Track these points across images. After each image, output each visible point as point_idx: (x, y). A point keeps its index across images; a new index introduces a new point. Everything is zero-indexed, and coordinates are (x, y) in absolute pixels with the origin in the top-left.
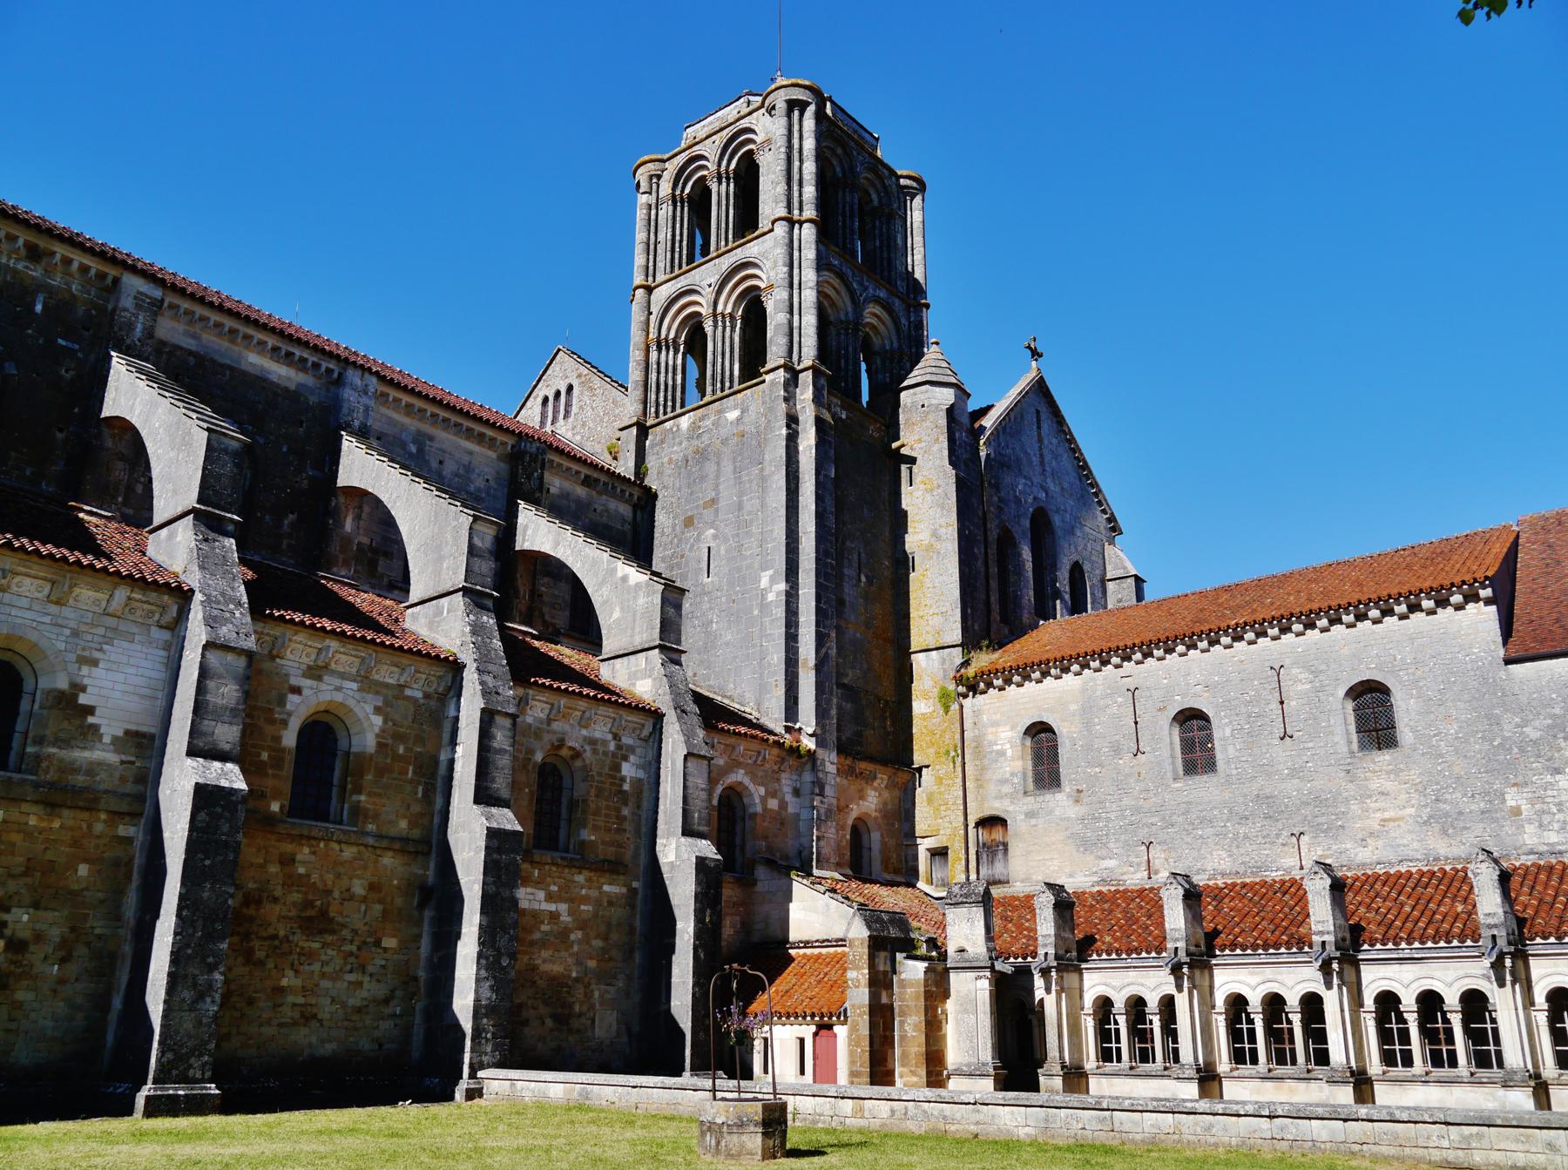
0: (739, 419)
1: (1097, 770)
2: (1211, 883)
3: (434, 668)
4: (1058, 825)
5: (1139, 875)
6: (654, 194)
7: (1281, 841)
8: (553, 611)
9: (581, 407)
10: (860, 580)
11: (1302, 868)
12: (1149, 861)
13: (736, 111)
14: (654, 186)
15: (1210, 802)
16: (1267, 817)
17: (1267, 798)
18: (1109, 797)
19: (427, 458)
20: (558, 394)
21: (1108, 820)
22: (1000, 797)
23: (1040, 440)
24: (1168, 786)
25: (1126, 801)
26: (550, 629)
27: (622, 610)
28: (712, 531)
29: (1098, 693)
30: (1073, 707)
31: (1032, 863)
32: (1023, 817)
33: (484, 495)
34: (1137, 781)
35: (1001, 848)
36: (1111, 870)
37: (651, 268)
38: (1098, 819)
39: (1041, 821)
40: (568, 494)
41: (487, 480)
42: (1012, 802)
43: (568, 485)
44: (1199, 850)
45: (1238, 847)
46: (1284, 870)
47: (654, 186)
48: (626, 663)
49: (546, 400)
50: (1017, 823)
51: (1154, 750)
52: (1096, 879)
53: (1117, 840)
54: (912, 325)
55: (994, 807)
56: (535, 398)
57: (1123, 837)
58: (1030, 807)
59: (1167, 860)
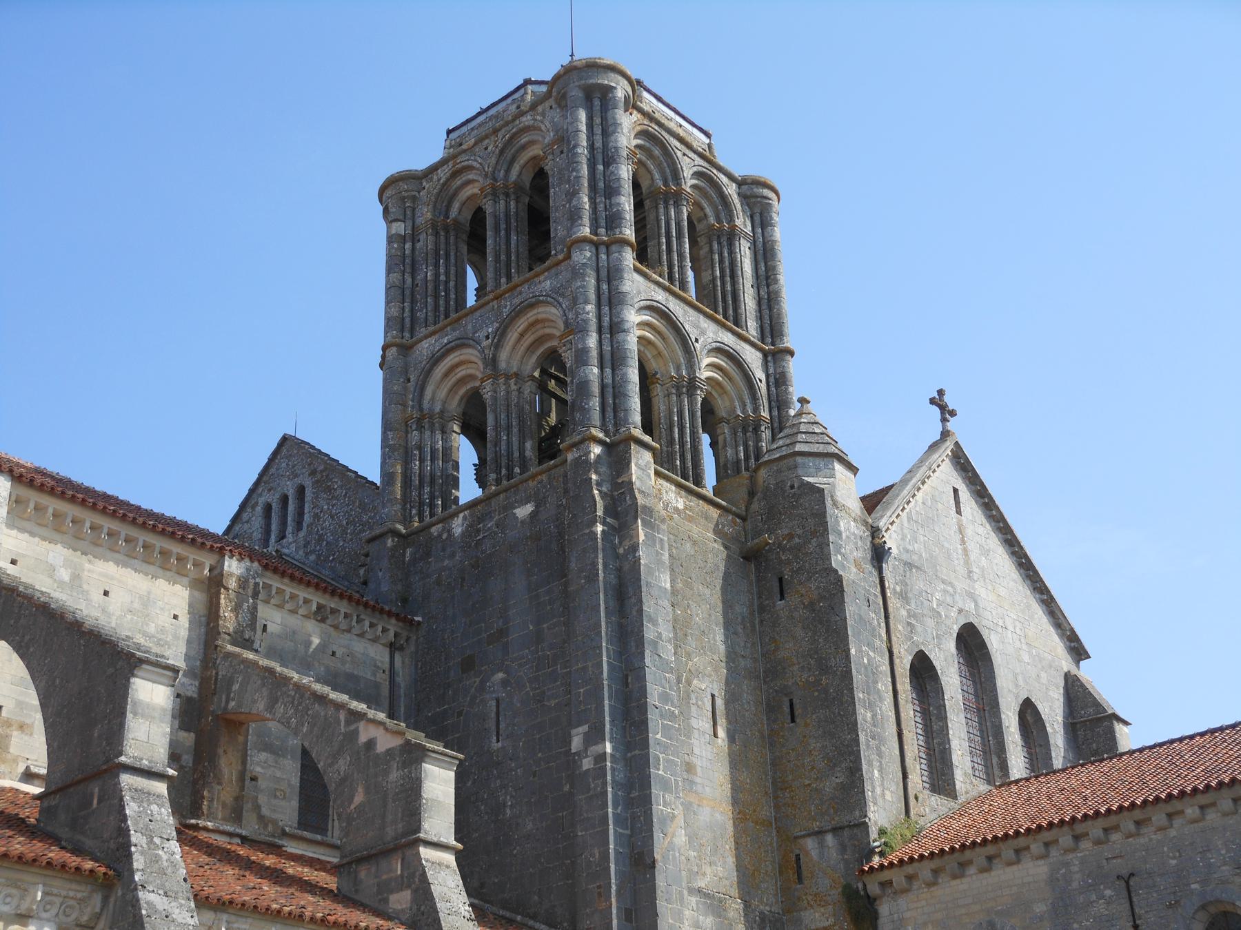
0: (534, 515)
3: (74, 886)
6: (409, 223)
8: (274, 802)
9: (316, 516)
10: (715, 735)
13: (514, 106)
14: (409, 213)
19: (85, 587)
20: (284, 500)
23: (961, 530)
26: (270, 828)
27: (367, 791)
28: (501, 675)
29: (1075, 885)
30: (1040, 908)
33: (169, 638)
37: (407, 321)
40: (294, 632)
41: (175, 617)
43: (294, 622)
47: (409, 213)
48: (373, 870)
49: (268, 508)
54: (772, 380)
56: (253, 508)
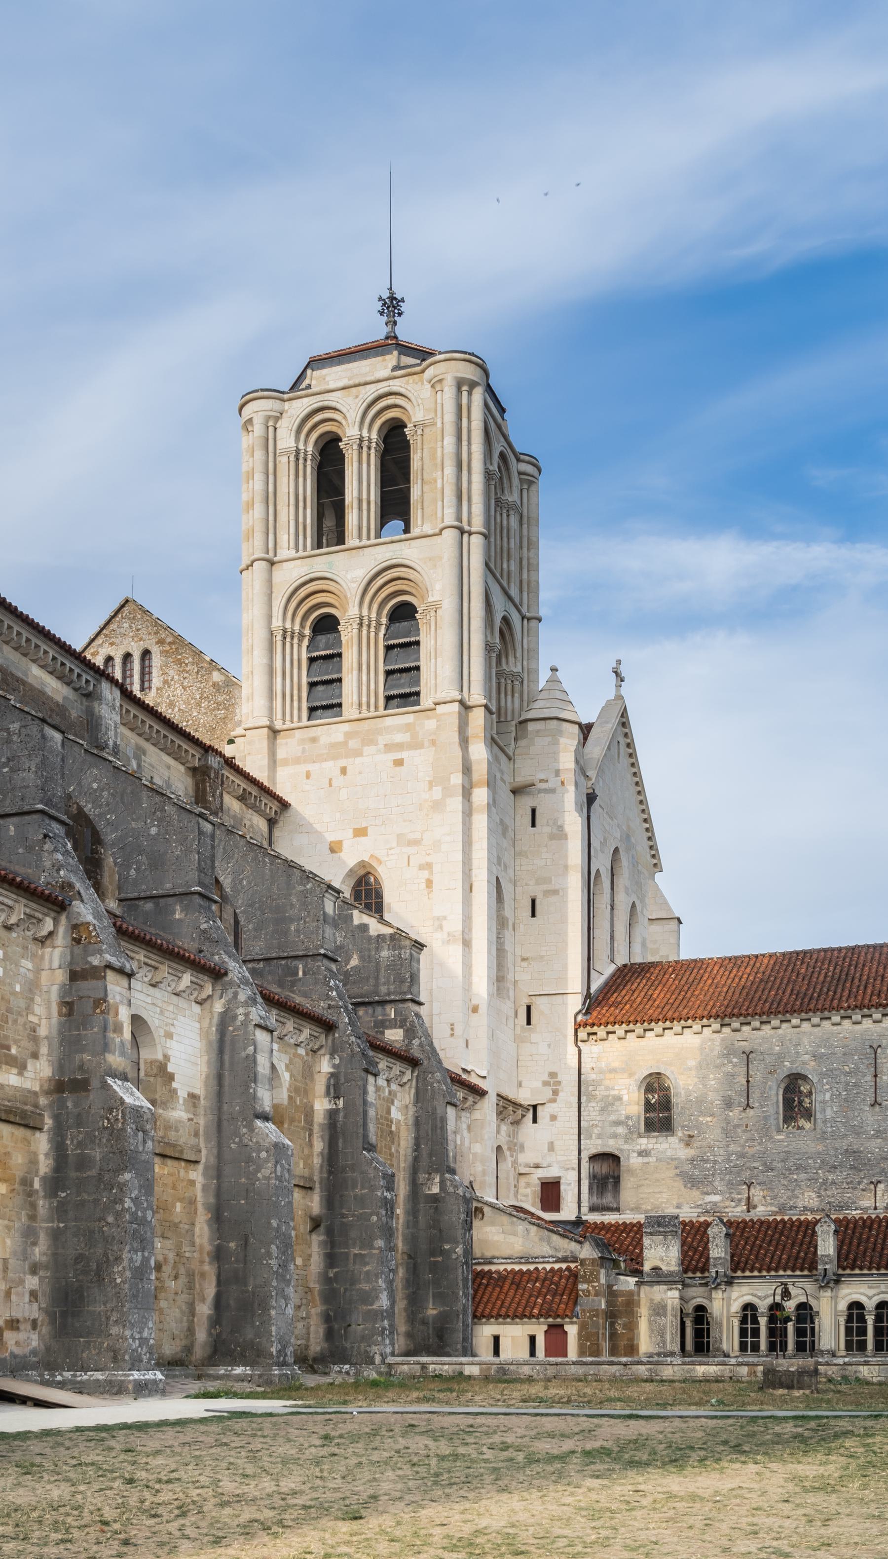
1: (709, 1119)
2: (802, 1218)
4: (668, 1164)
5: (739, 1209)
7: (861, 1187)
11: (875, 1208)
12: (749, 1198)
15: (806, 1153)
16: (852, 1167)
17: (855, 1152)
18: (717, 1143)
21: (715, 1162)
22: (615, 1136)
24: (771, 1137)
25: (733, 1148)
31: (642, 1196)
32: (635, 1155)
34: (744, 1131)
35: (611, 1180)
36: (715, 1204)
38: (707, 1161)
39: (652, 1159)
42: (626, 1142)
44: (793, 1191)
45: (826, 1190)
46: (861, 1209)
50: (632, 1161)
51: (762, 1106)
52: (700, 1210)
53: (722, 1180)
55: (611, 1146)
57: (727, 1177)
58: (644, 1147)
59: (764, 1197)
